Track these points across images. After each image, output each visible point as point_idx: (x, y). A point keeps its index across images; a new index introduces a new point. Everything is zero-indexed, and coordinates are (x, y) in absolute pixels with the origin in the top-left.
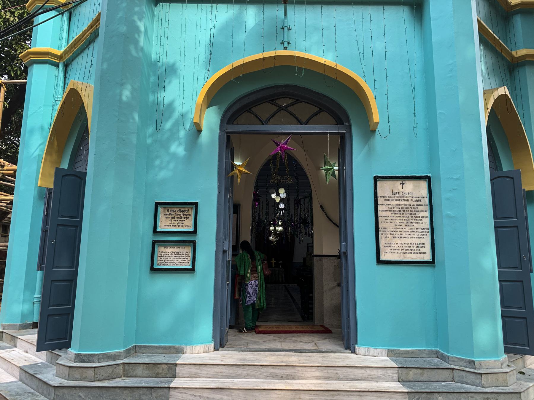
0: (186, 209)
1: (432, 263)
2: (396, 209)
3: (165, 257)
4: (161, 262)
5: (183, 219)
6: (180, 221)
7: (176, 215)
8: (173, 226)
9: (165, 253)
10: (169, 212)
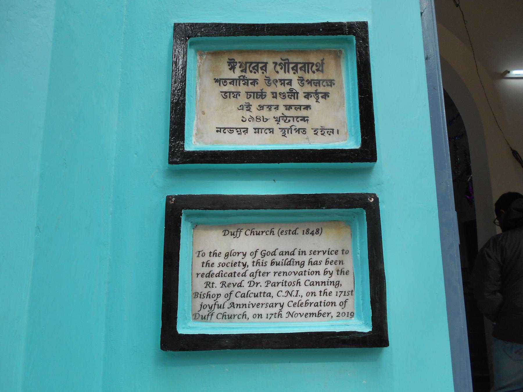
0: (314, 59)
3: (228, 280)
4: (210, 302)
5: (302, 101)
6: (289, 107)
7: (269, 85)
8: (257, 130)
9: (230, 259)
10: (238, 70)
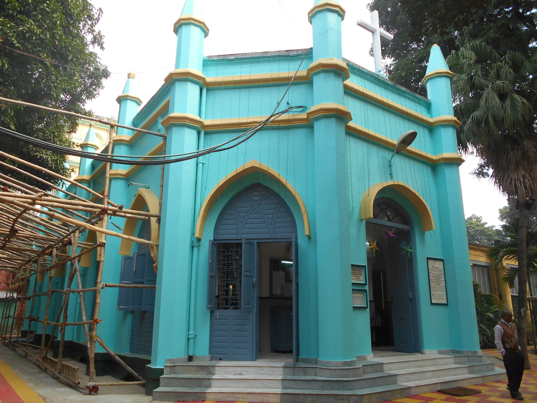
1: (446, 305)
2: (434, 276)
